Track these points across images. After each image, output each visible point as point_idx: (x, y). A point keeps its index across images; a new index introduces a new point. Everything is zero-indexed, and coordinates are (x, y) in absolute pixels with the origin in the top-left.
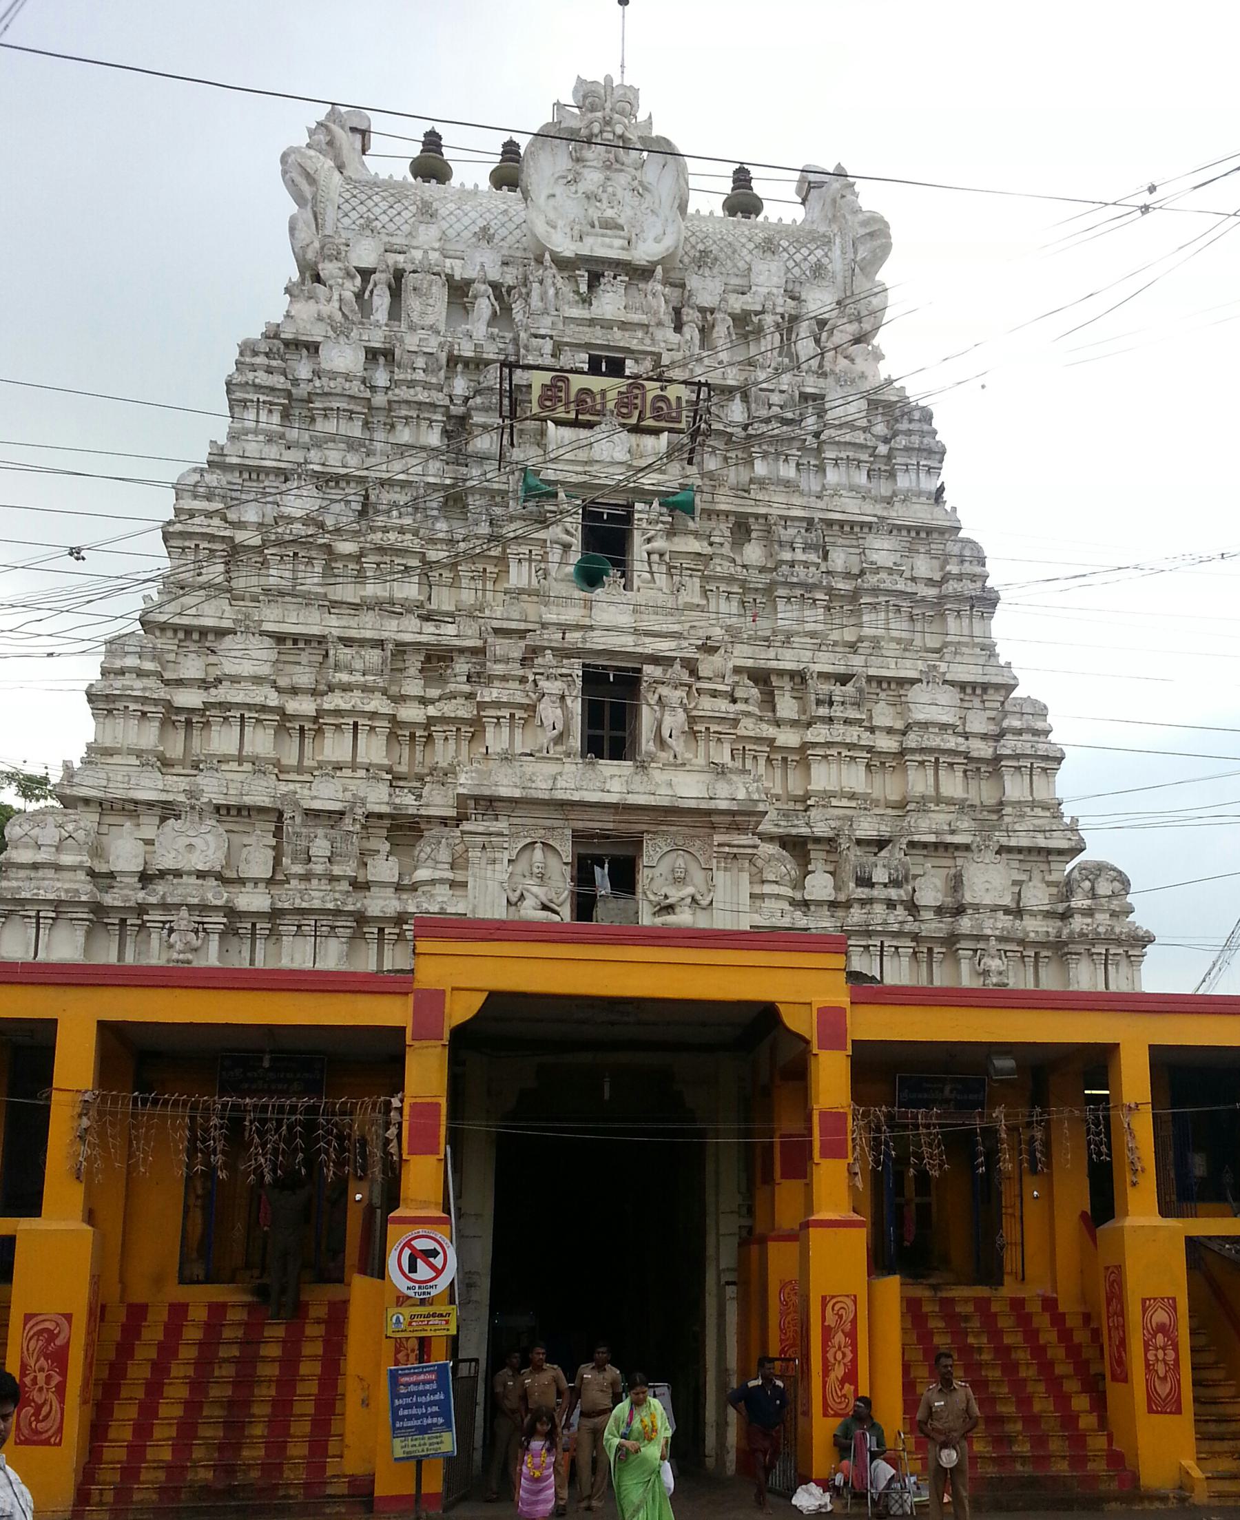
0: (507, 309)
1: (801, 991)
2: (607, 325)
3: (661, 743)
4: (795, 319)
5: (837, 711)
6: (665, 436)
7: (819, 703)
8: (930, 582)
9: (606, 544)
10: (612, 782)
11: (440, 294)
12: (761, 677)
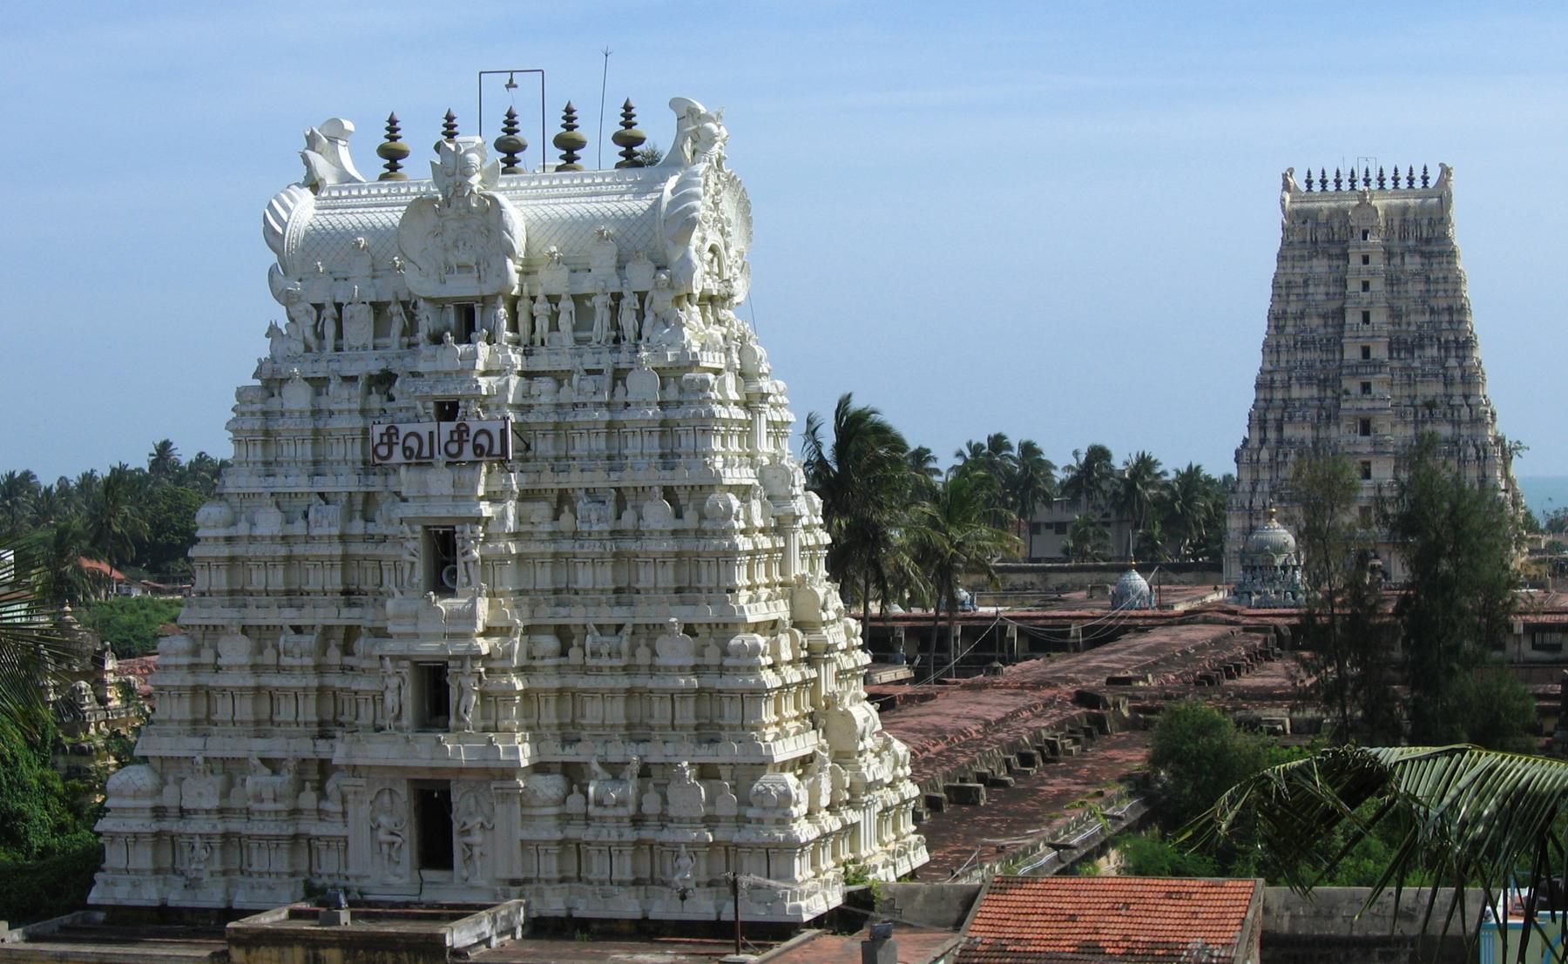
5: (604, 662)
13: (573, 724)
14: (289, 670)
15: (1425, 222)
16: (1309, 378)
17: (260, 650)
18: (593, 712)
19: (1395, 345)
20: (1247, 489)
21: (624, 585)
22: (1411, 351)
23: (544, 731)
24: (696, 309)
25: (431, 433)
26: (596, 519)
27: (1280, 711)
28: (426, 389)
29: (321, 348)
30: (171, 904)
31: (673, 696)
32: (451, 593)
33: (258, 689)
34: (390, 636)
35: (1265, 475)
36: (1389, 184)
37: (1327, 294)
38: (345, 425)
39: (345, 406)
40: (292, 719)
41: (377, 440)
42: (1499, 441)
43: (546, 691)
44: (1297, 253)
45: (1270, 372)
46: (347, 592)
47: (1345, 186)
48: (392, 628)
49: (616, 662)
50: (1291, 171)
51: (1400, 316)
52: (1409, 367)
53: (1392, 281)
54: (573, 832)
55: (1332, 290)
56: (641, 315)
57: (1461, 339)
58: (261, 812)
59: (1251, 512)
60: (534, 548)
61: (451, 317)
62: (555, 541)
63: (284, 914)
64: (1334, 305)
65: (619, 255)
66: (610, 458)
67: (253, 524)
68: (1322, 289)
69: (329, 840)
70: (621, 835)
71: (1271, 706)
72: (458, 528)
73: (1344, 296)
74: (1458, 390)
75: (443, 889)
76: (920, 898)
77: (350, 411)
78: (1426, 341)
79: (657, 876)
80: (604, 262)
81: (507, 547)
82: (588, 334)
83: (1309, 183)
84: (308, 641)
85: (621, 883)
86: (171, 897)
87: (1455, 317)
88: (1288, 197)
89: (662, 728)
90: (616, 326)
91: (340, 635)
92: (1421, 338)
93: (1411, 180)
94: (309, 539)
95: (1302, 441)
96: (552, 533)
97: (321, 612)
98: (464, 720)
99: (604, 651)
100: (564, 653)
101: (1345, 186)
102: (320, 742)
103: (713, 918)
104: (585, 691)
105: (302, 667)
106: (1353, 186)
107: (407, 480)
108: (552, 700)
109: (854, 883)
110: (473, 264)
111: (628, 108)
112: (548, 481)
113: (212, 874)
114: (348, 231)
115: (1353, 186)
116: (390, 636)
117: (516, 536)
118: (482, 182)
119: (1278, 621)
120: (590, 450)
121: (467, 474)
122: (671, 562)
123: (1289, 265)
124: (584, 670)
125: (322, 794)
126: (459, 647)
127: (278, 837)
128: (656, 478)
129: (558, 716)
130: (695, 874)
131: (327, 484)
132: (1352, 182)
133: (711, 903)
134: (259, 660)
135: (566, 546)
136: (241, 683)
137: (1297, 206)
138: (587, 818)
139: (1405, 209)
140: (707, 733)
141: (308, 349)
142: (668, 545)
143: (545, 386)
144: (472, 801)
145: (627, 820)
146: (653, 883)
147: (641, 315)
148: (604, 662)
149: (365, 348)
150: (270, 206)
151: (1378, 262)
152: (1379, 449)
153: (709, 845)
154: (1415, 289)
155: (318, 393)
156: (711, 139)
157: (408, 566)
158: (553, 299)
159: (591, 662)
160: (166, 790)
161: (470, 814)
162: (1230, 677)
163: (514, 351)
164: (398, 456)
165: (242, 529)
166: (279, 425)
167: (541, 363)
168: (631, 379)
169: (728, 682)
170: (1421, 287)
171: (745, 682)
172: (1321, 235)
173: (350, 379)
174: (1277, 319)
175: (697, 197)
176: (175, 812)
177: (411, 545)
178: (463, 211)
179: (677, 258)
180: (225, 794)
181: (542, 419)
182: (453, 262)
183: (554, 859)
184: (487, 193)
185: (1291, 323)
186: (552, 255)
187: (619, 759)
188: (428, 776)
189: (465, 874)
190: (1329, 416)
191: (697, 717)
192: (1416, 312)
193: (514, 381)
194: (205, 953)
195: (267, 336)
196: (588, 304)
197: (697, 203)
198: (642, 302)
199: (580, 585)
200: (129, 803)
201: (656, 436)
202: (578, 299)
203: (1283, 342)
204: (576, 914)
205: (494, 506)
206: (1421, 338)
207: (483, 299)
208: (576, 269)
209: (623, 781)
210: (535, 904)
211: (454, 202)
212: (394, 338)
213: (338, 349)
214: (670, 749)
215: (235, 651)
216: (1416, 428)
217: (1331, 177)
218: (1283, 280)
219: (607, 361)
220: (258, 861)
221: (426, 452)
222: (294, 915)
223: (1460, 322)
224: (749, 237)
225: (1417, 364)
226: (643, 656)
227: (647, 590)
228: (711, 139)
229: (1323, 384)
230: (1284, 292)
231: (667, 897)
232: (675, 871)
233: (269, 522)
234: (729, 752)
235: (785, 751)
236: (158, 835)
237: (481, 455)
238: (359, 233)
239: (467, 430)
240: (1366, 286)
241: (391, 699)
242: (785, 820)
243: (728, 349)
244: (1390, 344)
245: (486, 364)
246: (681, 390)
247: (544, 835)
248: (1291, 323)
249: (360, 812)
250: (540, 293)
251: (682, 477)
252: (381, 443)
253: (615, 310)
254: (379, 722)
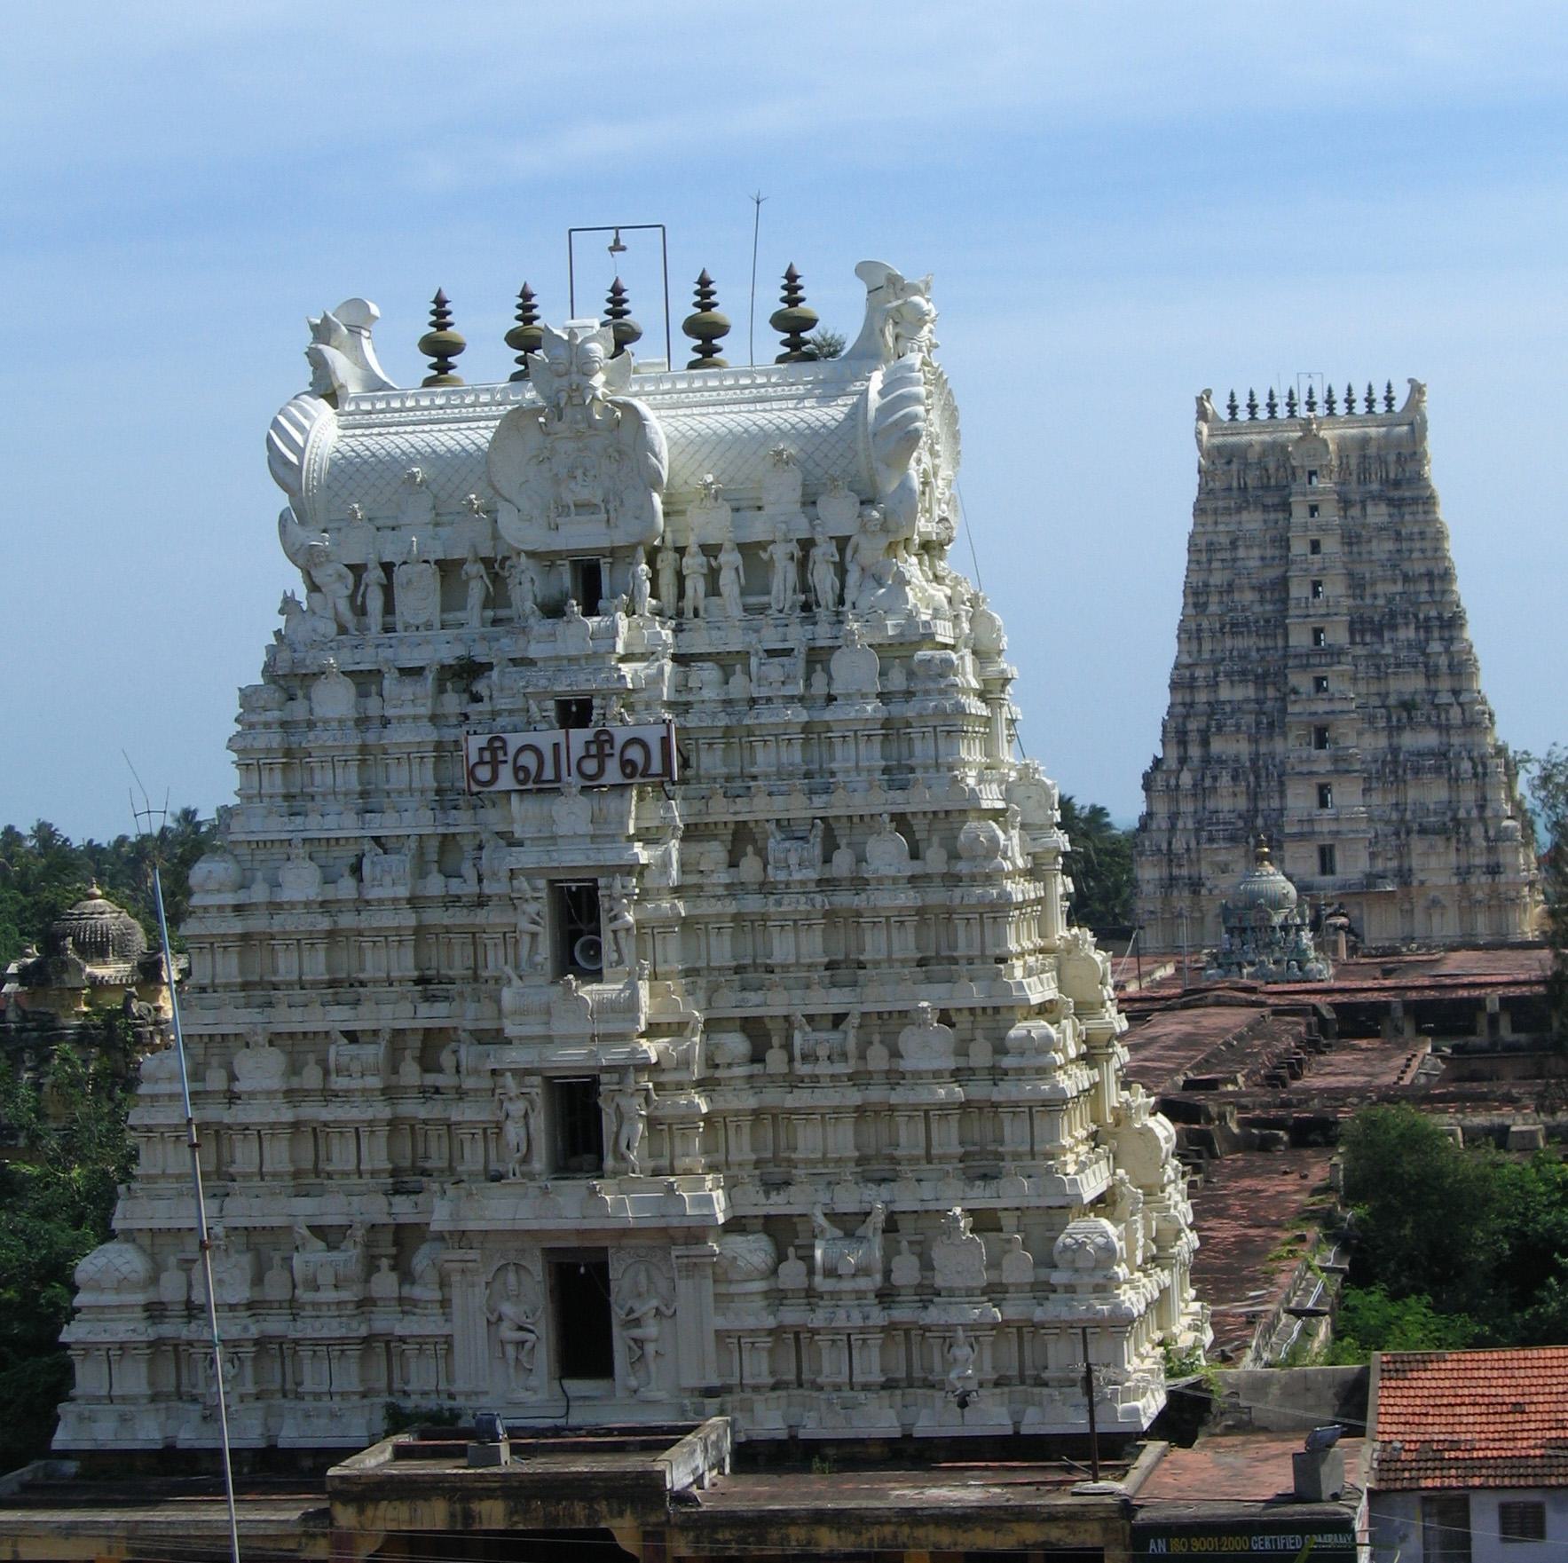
5: (823, 1068)
11: (430, 579)
13: (776, 1160)
14: (344, 1096)
15: (1392, 458)
16: (1244, 673)
17: (294, 1069)
18: (807, 1141)
19: (1360, 626)
20: (1164, 826)
21: (841, 957)
22: (1378, 632)
23: (734, 1171)
24: (914, 560)
25: (556, 746)
26: (796, 864)
27: (1446, 1118)
28: (543, 682)
29: (363, 629)
30: (180, 1445)
31: (927, 1113)
32: (597, 976)
33: (296, 1125)
34: (509, 1042)
35: (1187, 806)
36: (1341, 409)
37: (1263, 558)
38: (410, 737)
39: (409, 710)
40: (352, 1166)
41: (474, 758)
42: (1501, 751)
43: (737, 1113)
44: (1220, 504)
45: (1189, 666)
46: (421, 981)
47: (1282, 412)
48: (510, 1030)
49: (841, 1068)
50: (1208, 393)
51: (1363, 587)
52: (1377, 655)
53: (1350, 539)
54: (792, 1315)
55: (1269, 553)
56: (841, 571)
57: (1447, 615)
58: (316, 1305)
59: (1171, 857)
60: (708, 908)
61: (566, 578)
62: (733, 896)
63: (388, 1455)
64: (1272, 573)
65: (804, 485)
66: (808, 775)
67: (275, 885)
68: (1256, 552)
69: (422, 1341)
70: (866, 1318)
71: (1434, 1111)
72: (601, 882)
73: (1286, 560)
74: (1444, 684)
75: (603, 1406)
76: (1275, 1390)
77: (416, 718)
78: (1400, 620)
79: (918, 1373)
80: (783, 496)
81: (673, 906)
82: (764, 599)
83: (1233, 409)
84: (372, 1053)
85: (866, 1387)
86: (182, 1435)
87: (1437, 586)
88: (1205, 429)
89: (913, 1160)
90: (805, 587)
91: (415, 1042)
92: (1392, 614)
93: (1370, 402)
94: (361, 905)
95: (1237, 759)
96: (727, 886)
97: (387, 1010)
98: (624, 1158)
99: (822, 1052)
100: (757, 1057)
101: (1282, 412)
102: (397, 1199)
103: (1009, 1431)
104: (795, 1111)
105: (364, 1090)
106: (1292, 412)
107: (523, 814)
108: (746, 1130)
109: (1182, 1374)
110: (598, 500)
111: (791, 276)
112: (722, 811)
113: (242, 1398)
114: (395, 460)
115: (1292, 412)
116: (509, 1042)
117: (678, 891)
118: (607, 383)
119: (1314, 999)
120: (780, 766)
121: (612, 803)
122: (912, 922)
123: (1210, 520)
124: (793, 1082)
125: (406, 1275)
126: (615, 1054)
127: (343, 1341)
128: (885, 802)
129: (754, 1150)
130: (978, 1369)
131: (386, 825)
132: (1291, 405)
133: (1004, 1410)
134: (295, 1083)
135: (753, 904)
136: (272, 1117)
137: (1217, 441)
138: (811, 1294)
139: (1365, 441)
140: (982, 1166)
141: (343, 630)
142: (907, 898)
143: (707, 674)
144: (642, 1278)
145: (872, 1296)
146: (911, 1386)
147: (841, 571)
148: (823, 1068)
149: (429, 626)
150: (276, 425)
151: (1330, 513)
152: (1342, 766)
153: (995, 1326)
154: (1382, 548)
155: (363, 694)
156: (920, 318)
157: (526, 939)
158: (710, 550)
159: (802, 1069)
160: (165, 1277)
161: (639, 1295)
162: (1296, 1076)
163: (663, 624)
164: (506, 780)
165: (259, 893)
166: (312, 740)
167: (699, 642)
168: (838, 663)
169: (1007, 1091)
170: (1390, 546)
171: (1035, 1089)
172: (1252, 479)
173: (416, 672)
174: (1196, 593)
175: (916, 399)
176: (179, 1309)
177: (532, 908)
178: (582, 426)
179: (893, 486)
180: (258, 1280)
181: (707, 722)
182: (569, 499)
183: (764, 1354)
184: (620, 398)
185: (1214, 599)
186: (707, 486)
187: (852, 1207)
188: (574, 1243)
189: (633, 1382)
190: (1273, 725)
191: (962, 1143)
192: (1384, 580)
193: (668, 666)
194: (295, 1515)
195: (281, 612)
196: (764, 556)
197: (920, 409)
198: (842, 551)
199: (778, 957)
200: (110, 1298)
201: (877, 741)
202: (749, 550)
203: (1205, 625)
204: (803, 1434)
205: (651, 848)
206: (1392, 614)
207: (613, 552)
208: (742, 505)
209: (861, 1239)
210: (743, 1423)
211: (568, 412)
212: (473, 614)
213: (388, 629)
214: (927, 1191)
215: (261, 1071)
216: (1390, 736)
217: (1262, 400)
218: (1202, 541)
219: (797, 636)
220: (312, 1377)
221: (549, 773)
222: (401, 1453)
223: (1444, 592)
224: (956, 461)
225: (1388, 650)
226: (878, 1058)
227: (877, 964)
228: (920, 318)
229: (1261, 681)
230: (1204, 557)
231: (939, 1404)
232: (949, 1364)
233: (301, 883)
234: (1015, 1191)
235: (1093, 1184)
236: (156, 1344)
237: (631, 776)
238: (412, 462)
239: (611, 741)
240: (1315, 547)
241: (513, 1132)
242: (1106, 1287)
243: (957, 617)
244: (1352, 623)
245: (626, 645)
246: (911, 675)
247: (750, 1322)
248: (1214, 599)
249: (470, 1299)
250: (692, 542)
251: (918, 800)
252: (481, 762)
253: (803, 564)
254: (493, 1166)
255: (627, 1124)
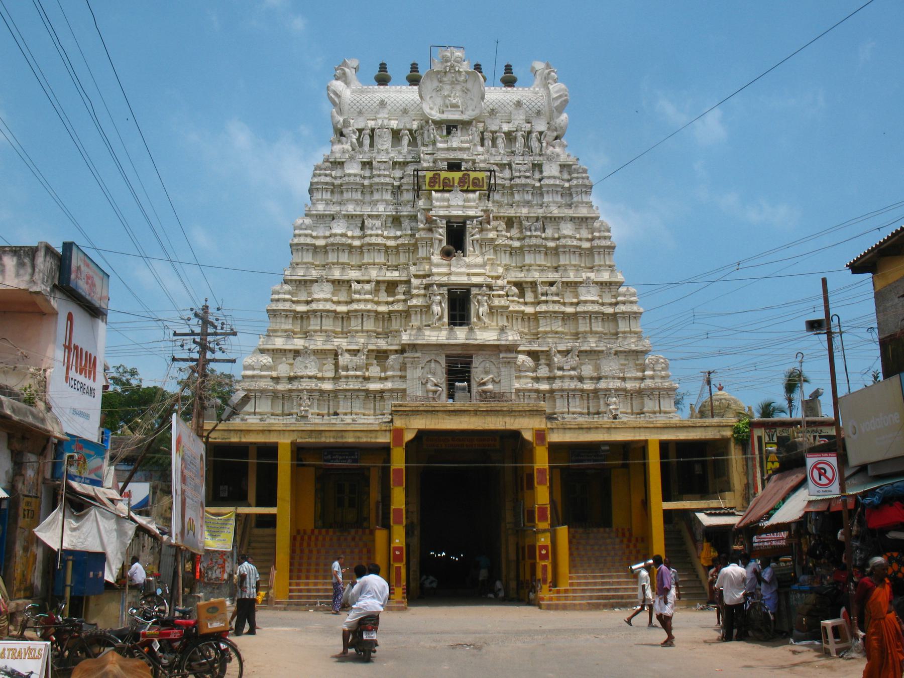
0: (414, 139)
1: (527, 427)
2: (454, 150)
3: (479, 318)
4: (530, 133)
5: (549, 298)
6: (478, 193)
7: (542, 294)
8: (588, 240)
9: (457, 238)
10: (461, 335)
12: (519, 285)
157: (437, 242)
255: (479, 308)
